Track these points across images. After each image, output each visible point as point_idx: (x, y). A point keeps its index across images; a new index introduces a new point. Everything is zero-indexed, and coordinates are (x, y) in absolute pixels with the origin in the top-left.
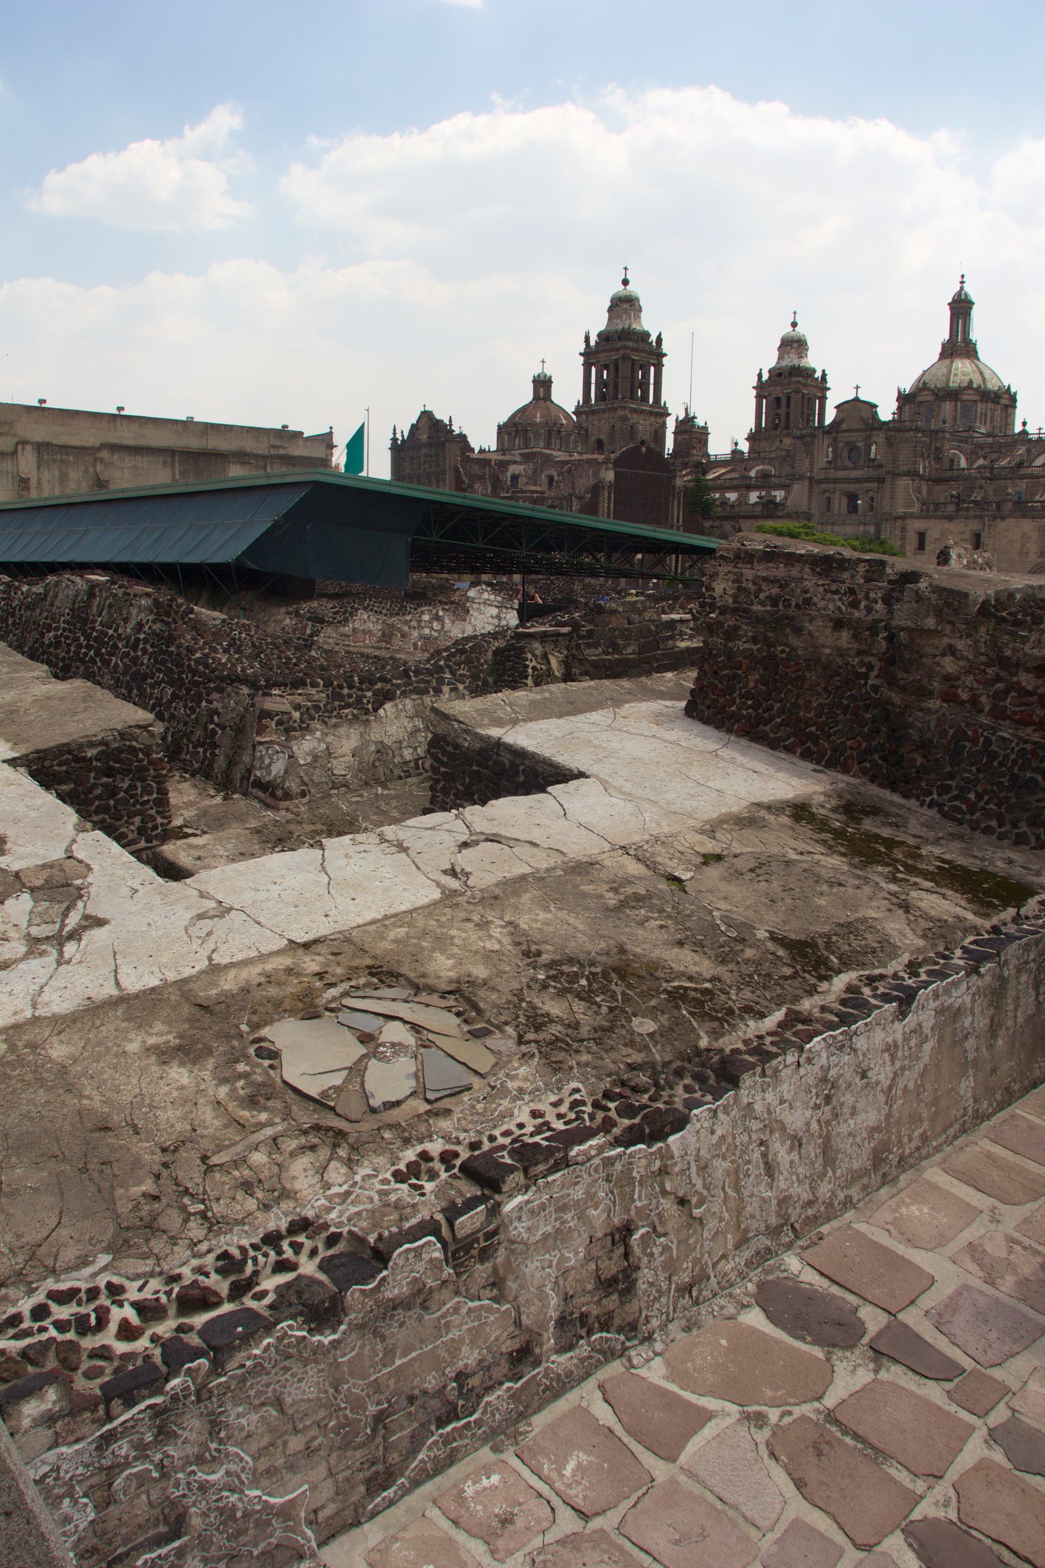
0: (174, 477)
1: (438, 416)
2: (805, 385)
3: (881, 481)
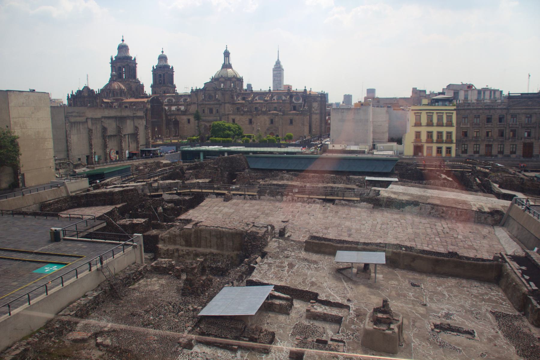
0: (116, 125)
1: (91, 88)
2: (169, 71)
3: (221, 105)
